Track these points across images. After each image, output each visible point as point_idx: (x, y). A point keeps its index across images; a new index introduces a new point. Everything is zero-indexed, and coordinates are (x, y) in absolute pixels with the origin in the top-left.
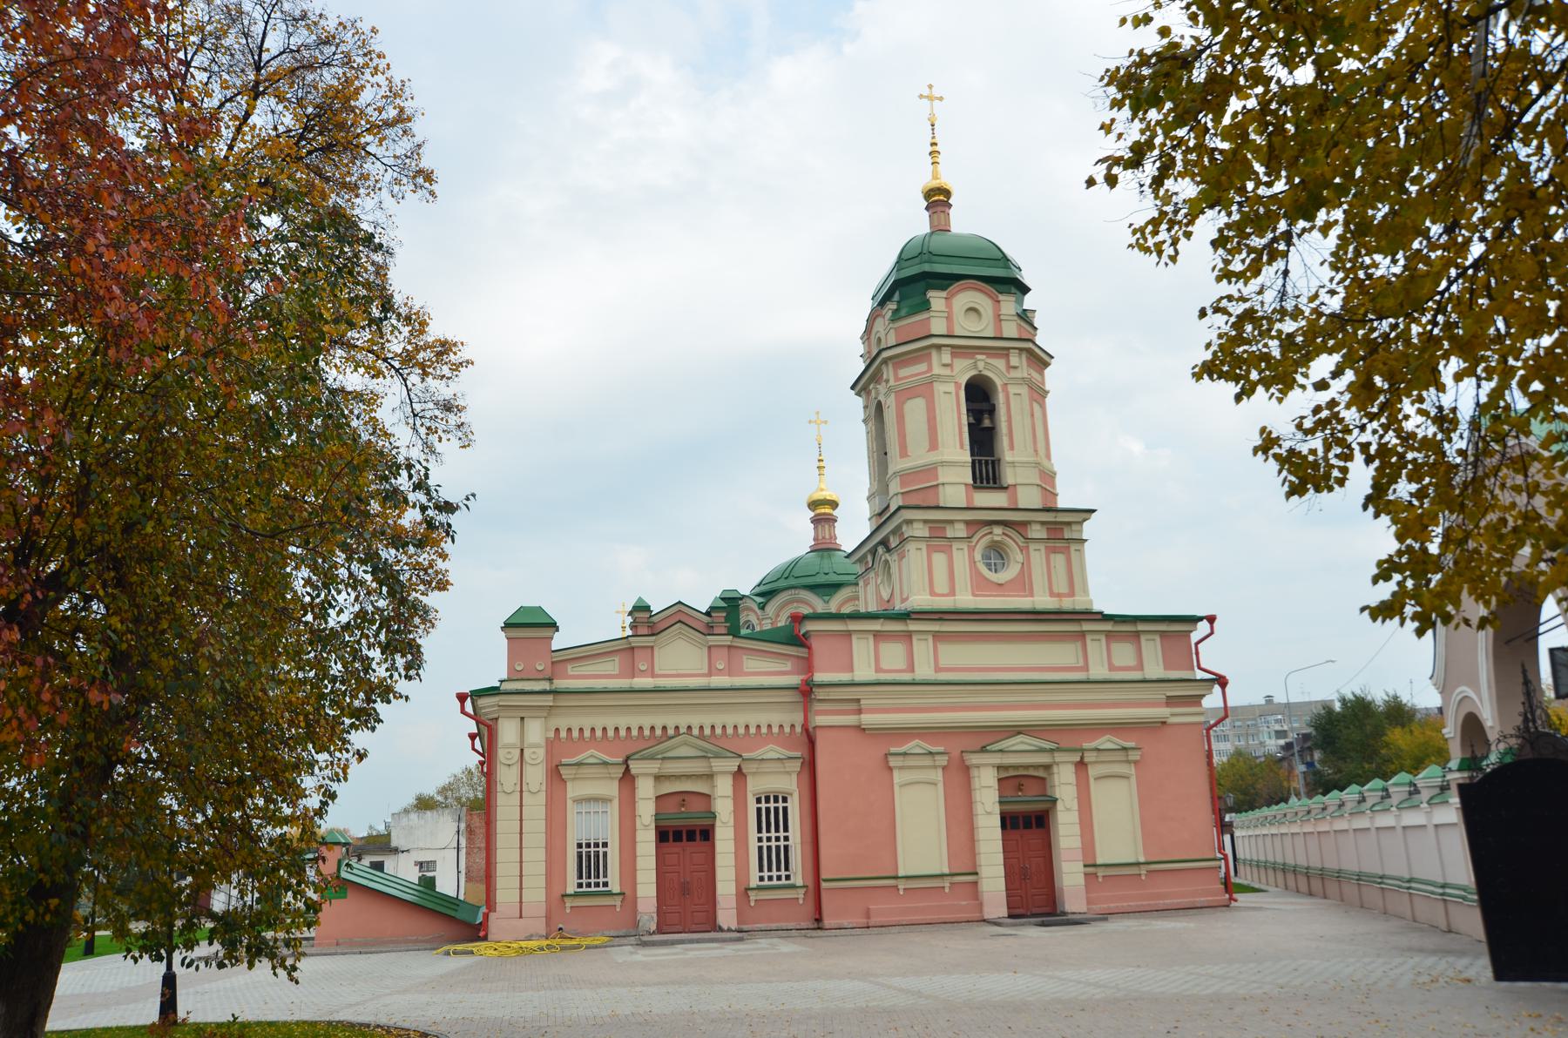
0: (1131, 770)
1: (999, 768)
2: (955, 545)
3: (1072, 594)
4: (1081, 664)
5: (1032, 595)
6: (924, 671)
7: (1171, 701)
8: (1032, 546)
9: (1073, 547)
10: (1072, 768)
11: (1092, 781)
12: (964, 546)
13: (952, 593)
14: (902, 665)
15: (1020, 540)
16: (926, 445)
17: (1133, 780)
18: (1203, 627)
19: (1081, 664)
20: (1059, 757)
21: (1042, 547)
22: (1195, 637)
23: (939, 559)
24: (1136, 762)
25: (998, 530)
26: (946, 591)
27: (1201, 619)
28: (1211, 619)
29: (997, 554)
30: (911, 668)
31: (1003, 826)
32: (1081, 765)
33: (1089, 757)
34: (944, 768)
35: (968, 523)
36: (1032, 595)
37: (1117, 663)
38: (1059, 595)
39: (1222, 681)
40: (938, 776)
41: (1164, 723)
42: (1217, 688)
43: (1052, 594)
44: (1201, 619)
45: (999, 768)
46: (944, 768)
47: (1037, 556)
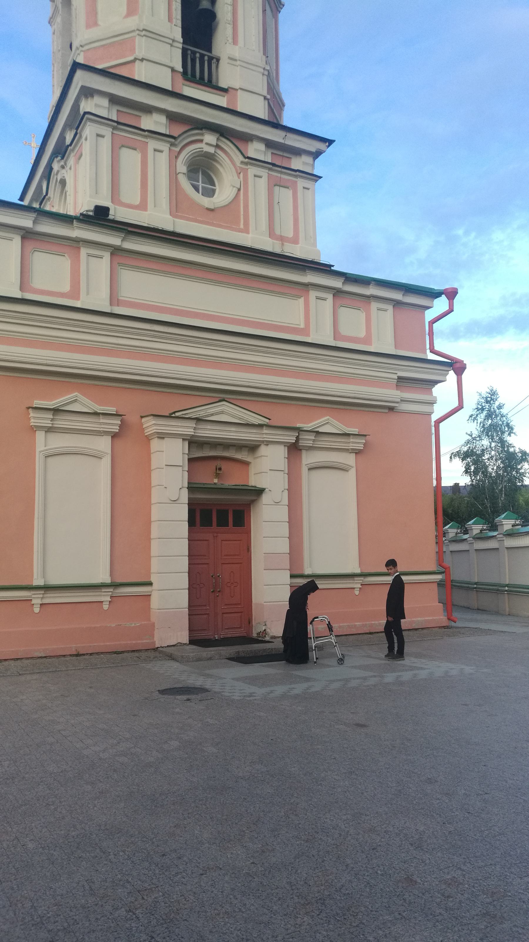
0: (350, 459)
1: (194, 443)
2: (152, 144)
3: (295, 240)
4: (302, 326)
5: (246, 230)
6: (97, 297)
7: (402, 382)
8: (252, 170)
9: (301, 183)
10: (281, 452)
11: (304, 470)
12: (164, 147)
13: (143, 206)
14: (66, 288)
15: (238, 158)
16: (124, 10)
17: (353, 473)
18: (440, 305)
19: (302, 326)
20: (266, 434)
21: (264, 173)
22: (430, 315)
23: (130, 159)
24: (357, 452)
25: (210, 138)
26: (137, 201)
27: (434, 294)
28: (451, 294)
29: (202, 170)
30: (75, 293)
31: (191, 522)
32: (294, 449)
33: (307, 440)
34: (115, 436)
35: (173, 118)
36: (246, 230)
37: (344, 331)
38: (282, 239)
39: (458, 367)
40: (104, 444)
41: (391, 409)
42: (452, 376)
43: (272, 234)
44: (436, 295)
45: (194, 443)
46: (115, 436)
47: (259, 183)
